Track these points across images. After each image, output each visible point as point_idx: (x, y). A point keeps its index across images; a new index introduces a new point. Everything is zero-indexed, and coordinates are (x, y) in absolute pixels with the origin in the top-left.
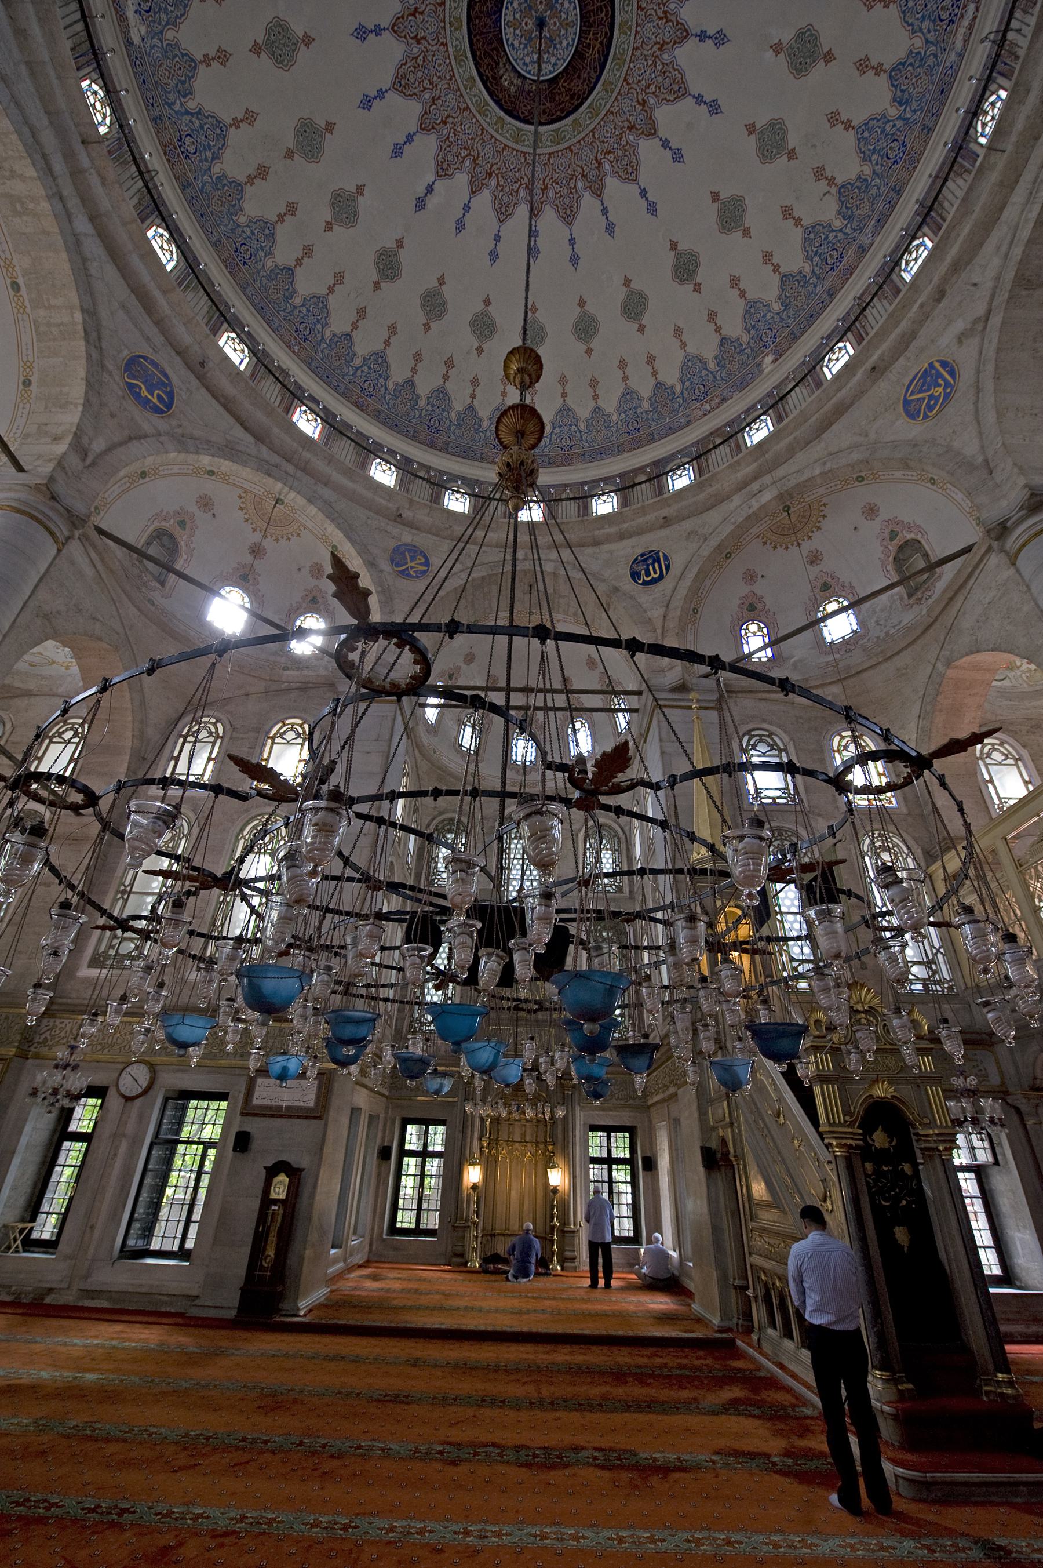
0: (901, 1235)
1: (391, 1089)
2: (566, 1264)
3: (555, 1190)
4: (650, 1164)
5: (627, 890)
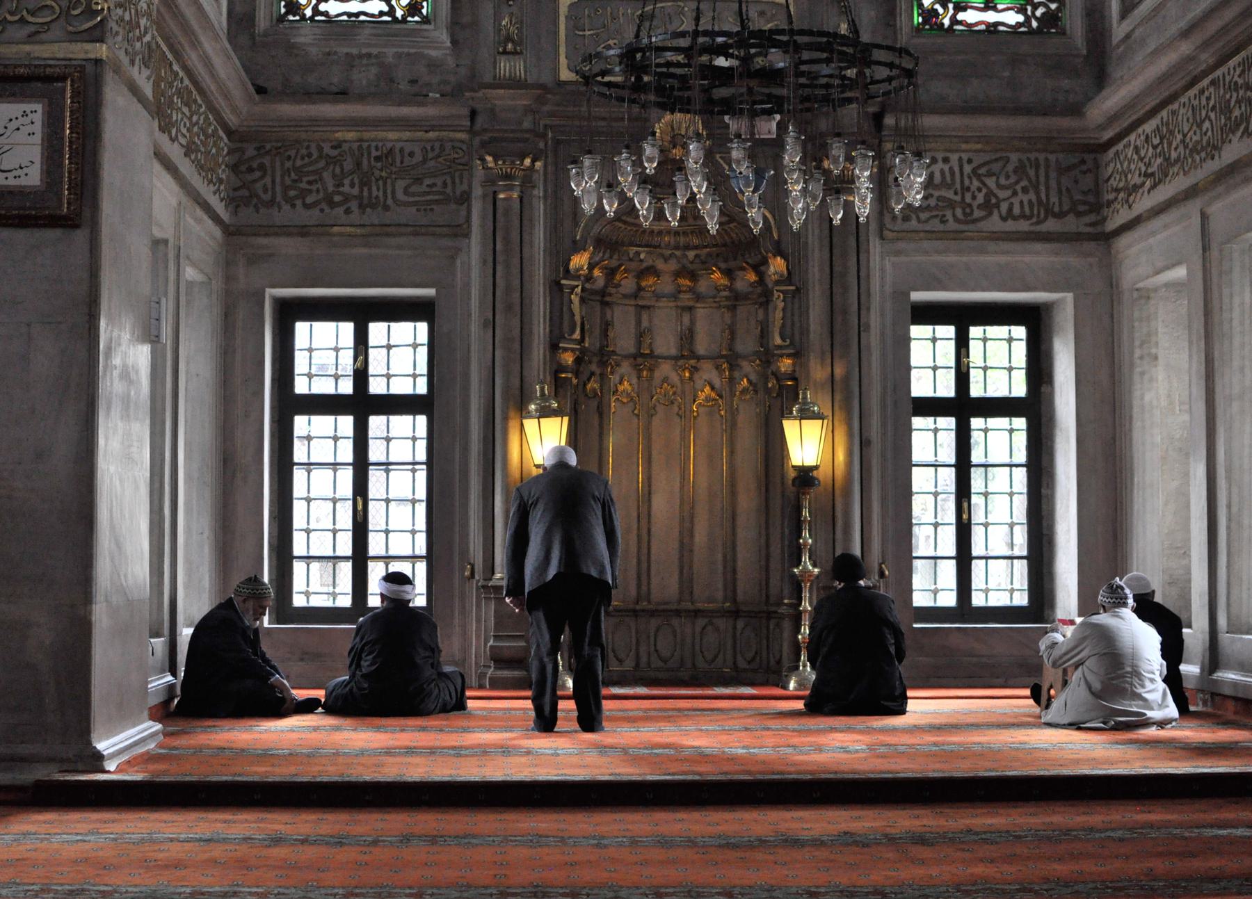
1: (234, 202)
3: (806, 476)
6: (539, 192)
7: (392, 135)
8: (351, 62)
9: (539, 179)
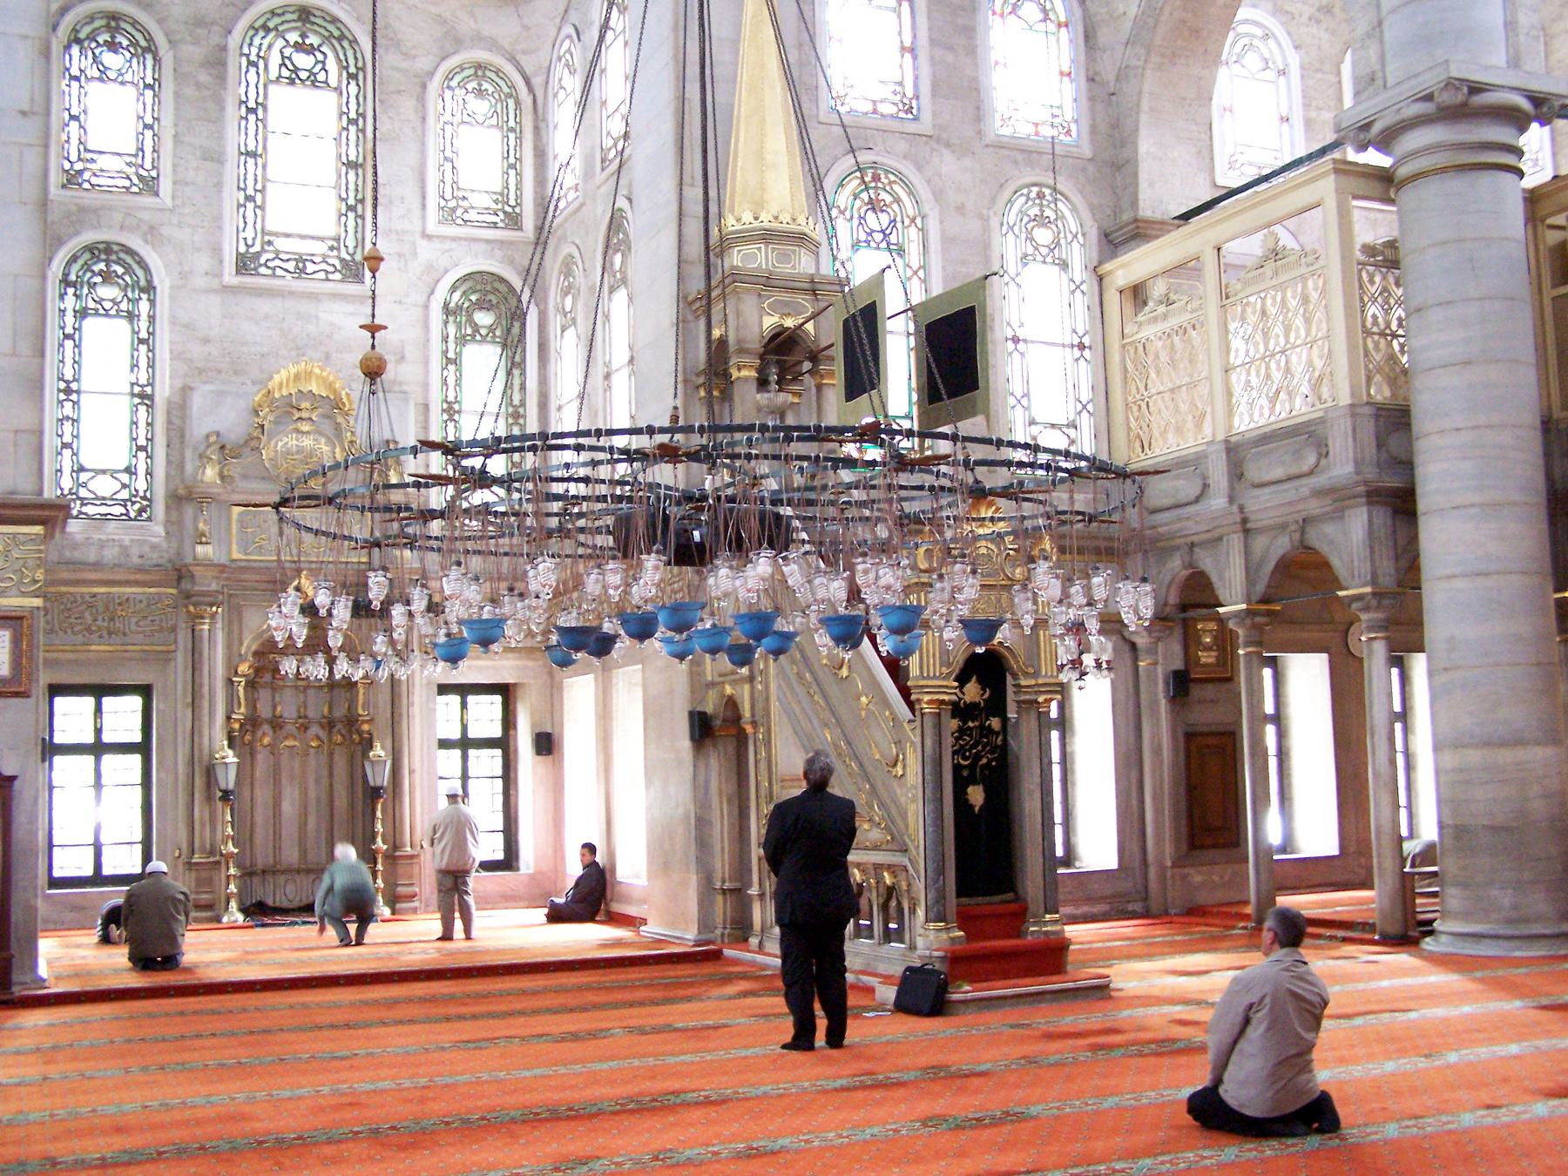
0: (976, 795)
2: (398, 906)
4: (546, 744)
5: (529, 223)
6: (219, 625)
7: (128, 590)
8: (102, 545)
9: (219, 618)
